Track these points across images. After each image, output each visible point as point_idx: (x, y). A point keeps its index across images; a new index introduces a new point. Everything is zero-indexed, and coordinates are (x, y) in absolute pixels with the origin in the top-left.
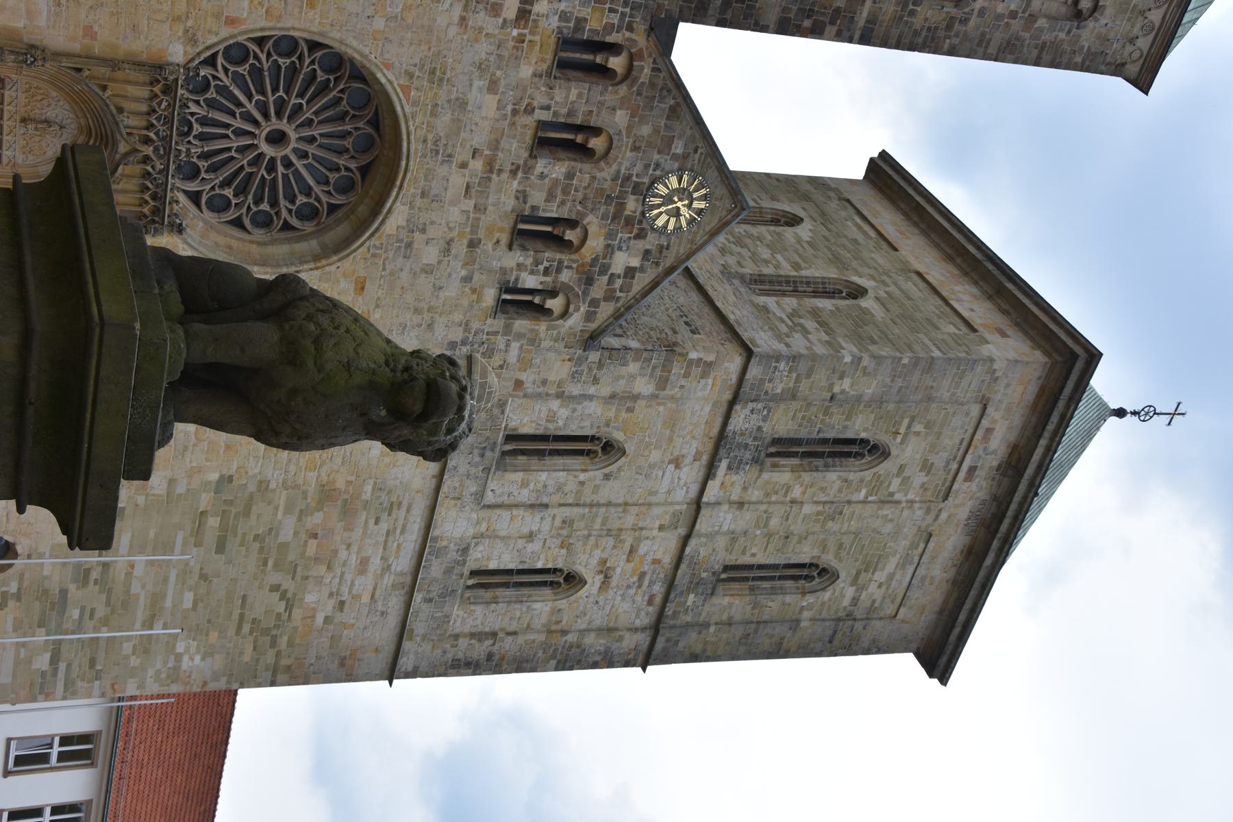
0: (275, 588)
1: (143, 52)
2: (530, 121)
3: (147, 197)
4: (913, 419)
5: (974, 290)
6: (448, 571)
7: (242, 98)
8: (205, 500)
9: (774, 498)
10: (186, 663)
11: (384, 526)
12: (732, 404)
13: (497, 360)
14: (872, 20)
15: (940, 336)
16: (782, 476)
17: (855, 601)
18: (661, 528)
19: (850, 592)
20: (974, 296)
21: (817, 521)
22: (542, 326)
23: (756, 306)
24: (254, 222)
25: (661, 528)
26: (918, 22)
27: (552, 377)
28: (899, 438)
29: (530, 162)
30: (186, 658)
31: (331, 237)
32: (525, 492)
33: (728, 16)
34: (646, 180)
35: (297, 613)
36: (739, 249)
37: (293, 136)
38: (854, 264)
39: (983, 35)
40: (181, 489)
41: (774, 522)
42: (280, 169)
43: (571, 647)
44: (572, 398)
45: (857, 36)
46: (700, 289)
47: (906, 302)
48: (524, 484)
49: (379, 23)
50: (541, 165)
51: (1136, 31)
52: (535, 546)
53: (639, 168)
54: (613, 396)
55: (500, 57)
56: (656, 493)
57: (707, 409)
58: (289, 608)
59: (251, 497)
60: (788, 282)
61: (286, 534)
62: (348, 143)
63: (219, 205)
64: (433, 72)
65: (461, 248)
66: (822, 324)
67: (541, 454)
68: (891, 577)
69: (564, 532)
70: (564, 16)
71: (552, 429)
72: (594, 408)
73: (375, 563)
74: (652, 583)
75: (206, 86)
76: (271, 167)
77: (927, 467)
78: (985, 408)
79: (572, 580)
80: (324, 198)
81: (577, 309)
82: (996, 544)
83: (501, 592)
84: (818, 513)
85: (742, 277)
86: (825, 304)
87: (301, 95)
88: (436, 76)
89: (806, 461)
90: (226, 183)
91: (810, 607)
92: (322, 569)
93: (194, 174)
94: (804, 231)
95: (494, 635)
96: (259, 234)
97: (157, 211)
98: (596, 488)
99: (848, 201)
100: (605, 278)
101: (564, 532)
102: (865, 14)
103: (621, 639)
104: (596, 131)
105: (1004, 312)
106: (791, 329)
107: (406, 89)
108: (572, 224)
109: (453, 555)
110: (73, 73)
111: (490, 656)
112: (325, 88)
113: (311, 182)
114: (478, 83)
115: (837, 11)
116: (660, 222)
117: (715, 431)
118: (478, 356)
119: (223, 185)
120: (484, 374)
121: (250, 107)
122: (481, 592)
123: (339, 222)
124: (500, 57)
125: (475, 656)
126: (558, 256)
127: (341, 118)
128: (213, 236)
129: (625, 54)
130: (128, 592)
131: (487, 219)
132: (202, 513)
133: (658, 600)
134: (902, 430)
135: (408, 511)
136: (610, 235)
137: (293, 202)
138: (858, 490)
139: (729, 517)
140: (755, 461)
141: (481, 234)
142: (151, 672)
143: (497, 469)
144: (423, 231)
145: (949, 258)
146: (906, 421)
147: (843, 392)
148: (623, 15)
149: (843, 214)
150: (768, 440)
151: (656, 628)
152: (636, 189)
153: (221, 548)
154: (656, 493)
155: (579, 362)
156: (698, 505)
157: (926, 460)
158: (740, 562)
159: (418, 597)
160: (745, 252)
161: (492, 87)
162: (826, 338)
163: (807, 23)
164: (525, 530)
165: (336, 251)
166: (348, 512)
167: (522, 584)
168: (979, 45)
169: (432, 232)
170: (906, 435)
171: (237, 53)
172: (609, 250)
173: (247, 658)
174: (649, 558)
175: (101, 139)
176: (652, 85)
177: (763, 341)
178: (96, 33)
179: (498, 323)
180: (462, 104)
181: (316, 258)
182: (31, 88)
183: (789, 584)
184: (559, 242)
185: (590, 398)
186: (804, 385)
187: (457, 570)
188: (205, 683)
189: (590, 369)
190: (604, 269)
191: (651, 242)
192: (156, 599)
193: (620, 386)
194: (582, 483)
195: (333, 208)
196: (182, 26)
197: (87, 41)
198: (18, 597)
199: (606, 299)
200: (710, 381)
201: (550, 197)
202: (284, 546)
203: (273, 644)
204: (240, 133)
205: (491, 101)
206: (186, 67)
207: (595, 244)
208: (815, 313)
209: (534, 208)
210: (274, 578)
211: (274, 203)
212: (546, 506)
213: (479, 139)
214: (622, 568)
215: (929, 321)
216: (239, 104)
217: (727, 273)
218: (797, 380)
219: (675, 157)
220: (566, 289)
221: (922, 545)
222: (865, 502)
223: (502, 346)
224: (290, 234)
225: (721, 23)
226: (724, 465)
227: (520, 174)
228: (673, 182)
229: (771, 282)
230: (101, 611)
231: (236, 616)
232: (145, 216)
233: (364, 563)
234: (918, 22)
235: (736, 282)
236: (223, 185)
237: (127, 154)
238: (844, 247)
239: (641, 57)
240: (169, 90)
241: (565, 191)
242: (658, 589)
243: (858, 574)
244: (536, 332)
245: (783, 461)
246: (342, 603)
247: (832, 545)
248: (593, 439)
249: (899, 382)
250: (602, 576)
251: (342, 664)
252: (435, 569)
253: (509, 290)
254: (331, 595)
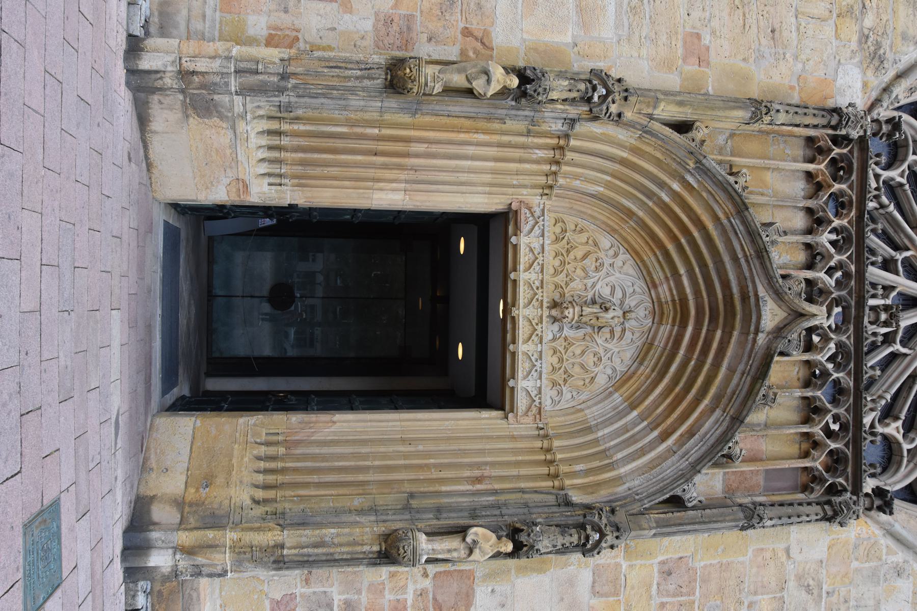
1: (792, 88)
3: (817, 430)
110: (675, 135)
175: (713, 319)
178: (708, 49)
182: (564, 231)
196: (856, 28)
197: (691, 68)
232: (819, 480)
237: (779, 331)
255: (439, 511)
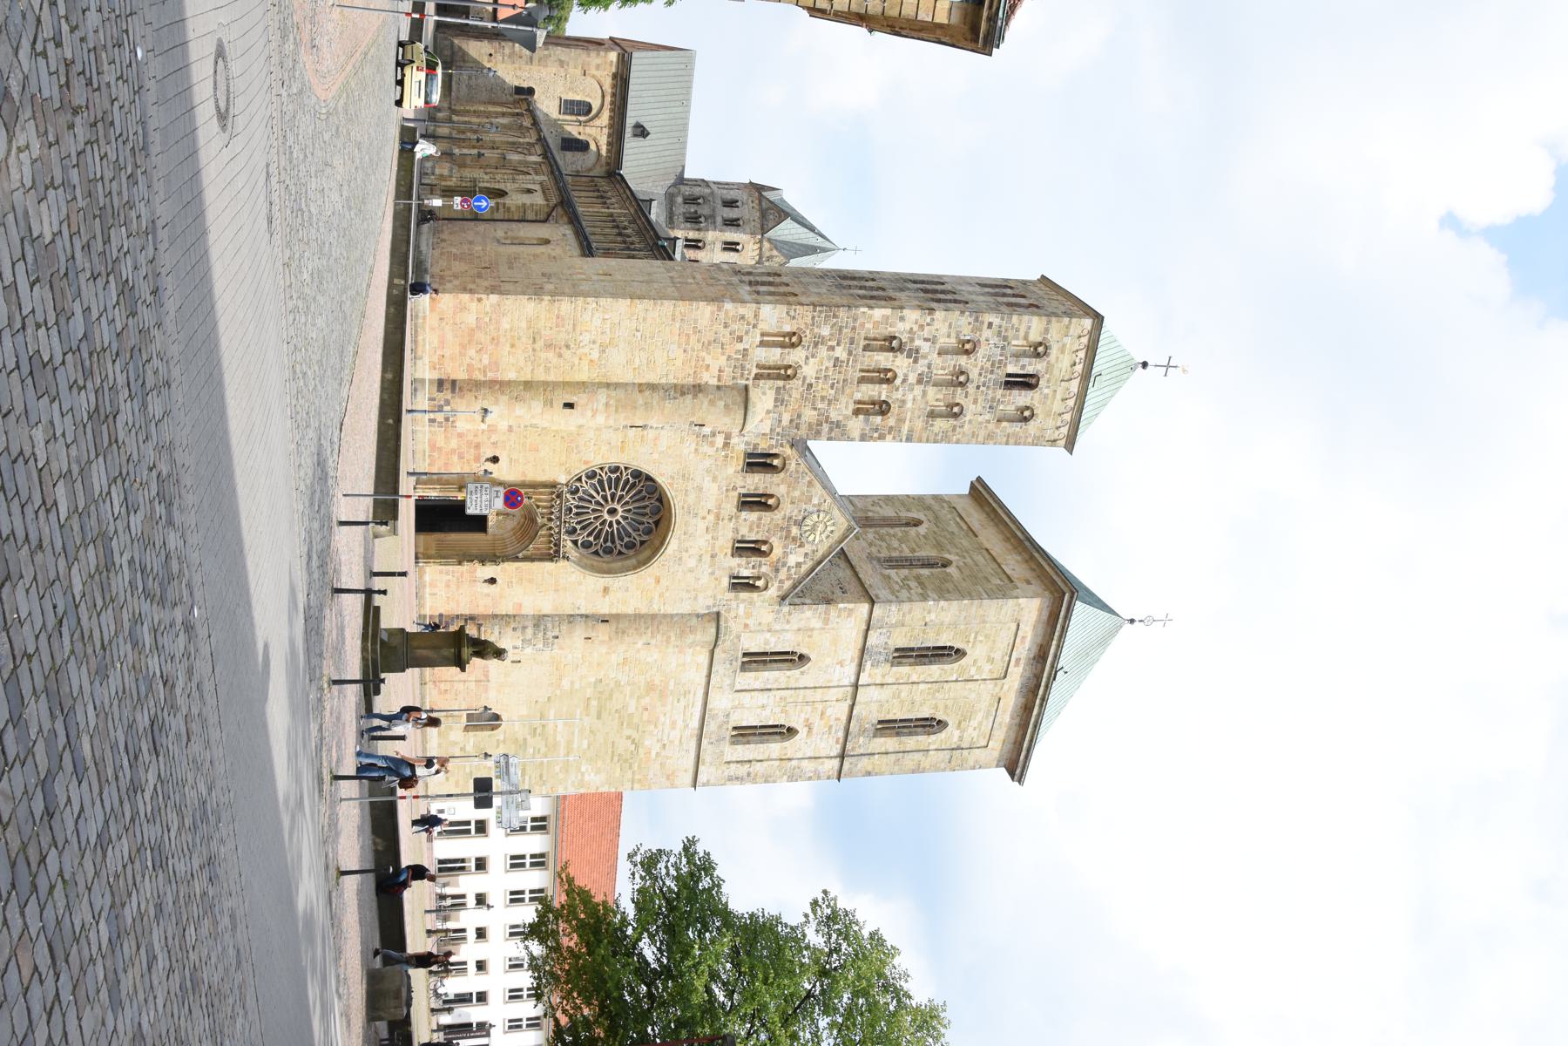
0: (628, 737)
2: (735, 494)
4: (977, 634)
5: (1019, 558)
6: (720, 727)
7: (595, 494)
8: (589, 692)
9: (901, 681)
10: (587, 778)
11: (683, 703)
12: (867, 630)
13: (733, 614)
14: (911, 431)
15: (990, 586)
16: (904, 670)
17: (961, 739)
18: (837, 700)
19: (957, 733)
20: (1018, 562)
21: (929, 694)
22: (755, 595)
23: (882, 574)
24: (604, 552)
25: (837, 700)
26: (936, 429)
27: (764, 621)
28: (970, 645)
29: (738, 514)
30: (586, 775)
31: (642, 557)
32: (758, 683)
33: (833, 435)
34: (800, 518)
35: (640, 750)
36: (880, 543)
37: (620, 510)
38: (949, 547)
39: (974, 432)
40: (577, 686)
41: (903, 695)
42: (615, 526)
43: (794, 769)
44: (777, 631)
45: (904, 439)
46: (852, 567)
47: (975, 568)
48: (756, 679)
49: (656, 456)
50: (744, 514)
51: (1059, 424)
52: (768, 711)
53: (796, 512)
54: (799, 630)
55: (717, 465)
56: (831, 681)
57: (854, 634)
58: (637, 748)
59: (612, 690)
60: (906, 560)
61: (632, 709)
62: (647, 510)
63: (586, 545)
64: (684, 476)
65: (707, 558)
66: (921, 584)
67: (765, 662)
68: (980, 724)
69: (782, 704)
70: (747, 443)
71: (769, 649)
72: (789, 636)
73: (680, 723)
74: (836, 731)
75: (577, 490)
76: (611, 525)
77: (990, 660)
78: (1018, 625)
79: (791, 731)
80: (638, 538)
81: (773, 585)
82: (1038, 702)
83: (751, 738)
84: (929, 689)
85: (879, 560)
86: (925, 572)
87: (623, 490)
88: (685, 477)
89: (918, 660)
90: (589, 535)
91: (934, 743)
92: (652, 727)
93: (573, 531)
94: (922, 529)
95: (750, 761)
96: (607, 558)
97: (557, 552)
98: (797, 680)
99: (954, 508)
100: (786, 569)
101: (782, 704)
102: (906, 428)
103: (823, 763)
104: (771, 496)
105: (1034, 570)
106: (901, 587)
107: (671, 485)
108: (765, 542)
109: (721, 718)
111: (749, 774)
112: (634, 485)
113: (631, 531)
114: (707, 479)
115: (891, 428)
116: (811, 538)
117: (859, 645)
118: (723, 612)
119: (588, 536)
120: (726, 621)
121: (599, 498)
122: (741, 738)
123: (645, 549)
124: (717, 465)
125: (741, 775)
126: (759, 559)
127: (643, 499)
128: (585, 560)
129: (781, 458)
130: (555, 739)
131: (718, 543)
132: (589, 699)
133: (841, 740)
134: (971, 640)
135: (694, 694)
136: (785, 547)
137: (622, 540)
138: (951, 675)
139: (877, 693)
140: (887, 661)
141: (717, 550)
142: (570, 782)
143: (741, 671)
144: (687, 551)
145: (1007, 540)
146: (973, 635)
147: (931, 621)
148: (777, 440)
149: (949, 516)
150: (893, 649)
151: (842, 756)
152: (796, 523)
153: (599, 717)
154: (831, 681)
155: (778, 612)
156: (856, 686)
157: (989, 656)
158: (887, 718)
159: (705, 742)
160: (884, 545)
161: (715, 479)
162: (920, 591)
163: (876, 435)
164: (760, 704)
165: (644, 564)
166: (663, 695)
167: (764, 734)
168: (973, 436)
169: (691, 551)
170: (974, 642)
171: (592, 475)
172: (786, 554)
173: (617, 775)
174: (833, 717)
176: (797, 472)
177: (883, 593)
179: (732, 595)
180: (700, 489)
181: (635, 568)
183: (920, 729)
184: (756, 551)
185: (787, 631)
186: (908, 617)
187: (725, 726)
188: (597, 788)
189: (784, 616)
190: (784, 564)
191: (808, 548)
192: (569, 743)
193: (802, 624)
194: (789, 677)
195: (642, 543)
198: (504, 742)
199: (788, 579)
200: (853, 619)
201: (751, 530)
202: (631, 715)
203: (630, 767)
204: (594, 510)
205: (714, 486)
206: (567, 485)
207: (777, 552)
208: (918, 578)
209: (742, 536)
210: (628, 732)
211: (613, 542)
212: (770, 690)
213: (711, 505)
214: (818, 725)
215: (986, 578)
216: (593, 497)
217: (870, 557)
218: (904, 615)
219: (814, 505)
220: (765, 575)
221: (996, 704)
222: (956, 681)
223: (735, 606)
224: (623, 557)
225: (829, 439)
226: (869, 663)
227: (734, 520)
228: (815, 517)
229: (897, 561)
230: (543, 750)
231: (610, 753)
233: (674, 723)
234: (936, 429)
235: (875, 562)
236: (588, 536)
238: (945, 537)
239: (789, 459)
240: (559, 496)
241: (758, 526)
242: (841, 734)
243: (960, 723)
244: (752, 598)
245: (904, 660)
246: (664, 745)
247: (941, 707)
248: (793, 653)
249: (964, 614)
250: (806, 729)
251: (668, 779)
252: (711, 726)
253: (735, 578)
254: (658, 741)
255: (470, 556)
